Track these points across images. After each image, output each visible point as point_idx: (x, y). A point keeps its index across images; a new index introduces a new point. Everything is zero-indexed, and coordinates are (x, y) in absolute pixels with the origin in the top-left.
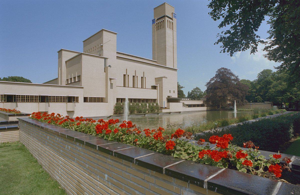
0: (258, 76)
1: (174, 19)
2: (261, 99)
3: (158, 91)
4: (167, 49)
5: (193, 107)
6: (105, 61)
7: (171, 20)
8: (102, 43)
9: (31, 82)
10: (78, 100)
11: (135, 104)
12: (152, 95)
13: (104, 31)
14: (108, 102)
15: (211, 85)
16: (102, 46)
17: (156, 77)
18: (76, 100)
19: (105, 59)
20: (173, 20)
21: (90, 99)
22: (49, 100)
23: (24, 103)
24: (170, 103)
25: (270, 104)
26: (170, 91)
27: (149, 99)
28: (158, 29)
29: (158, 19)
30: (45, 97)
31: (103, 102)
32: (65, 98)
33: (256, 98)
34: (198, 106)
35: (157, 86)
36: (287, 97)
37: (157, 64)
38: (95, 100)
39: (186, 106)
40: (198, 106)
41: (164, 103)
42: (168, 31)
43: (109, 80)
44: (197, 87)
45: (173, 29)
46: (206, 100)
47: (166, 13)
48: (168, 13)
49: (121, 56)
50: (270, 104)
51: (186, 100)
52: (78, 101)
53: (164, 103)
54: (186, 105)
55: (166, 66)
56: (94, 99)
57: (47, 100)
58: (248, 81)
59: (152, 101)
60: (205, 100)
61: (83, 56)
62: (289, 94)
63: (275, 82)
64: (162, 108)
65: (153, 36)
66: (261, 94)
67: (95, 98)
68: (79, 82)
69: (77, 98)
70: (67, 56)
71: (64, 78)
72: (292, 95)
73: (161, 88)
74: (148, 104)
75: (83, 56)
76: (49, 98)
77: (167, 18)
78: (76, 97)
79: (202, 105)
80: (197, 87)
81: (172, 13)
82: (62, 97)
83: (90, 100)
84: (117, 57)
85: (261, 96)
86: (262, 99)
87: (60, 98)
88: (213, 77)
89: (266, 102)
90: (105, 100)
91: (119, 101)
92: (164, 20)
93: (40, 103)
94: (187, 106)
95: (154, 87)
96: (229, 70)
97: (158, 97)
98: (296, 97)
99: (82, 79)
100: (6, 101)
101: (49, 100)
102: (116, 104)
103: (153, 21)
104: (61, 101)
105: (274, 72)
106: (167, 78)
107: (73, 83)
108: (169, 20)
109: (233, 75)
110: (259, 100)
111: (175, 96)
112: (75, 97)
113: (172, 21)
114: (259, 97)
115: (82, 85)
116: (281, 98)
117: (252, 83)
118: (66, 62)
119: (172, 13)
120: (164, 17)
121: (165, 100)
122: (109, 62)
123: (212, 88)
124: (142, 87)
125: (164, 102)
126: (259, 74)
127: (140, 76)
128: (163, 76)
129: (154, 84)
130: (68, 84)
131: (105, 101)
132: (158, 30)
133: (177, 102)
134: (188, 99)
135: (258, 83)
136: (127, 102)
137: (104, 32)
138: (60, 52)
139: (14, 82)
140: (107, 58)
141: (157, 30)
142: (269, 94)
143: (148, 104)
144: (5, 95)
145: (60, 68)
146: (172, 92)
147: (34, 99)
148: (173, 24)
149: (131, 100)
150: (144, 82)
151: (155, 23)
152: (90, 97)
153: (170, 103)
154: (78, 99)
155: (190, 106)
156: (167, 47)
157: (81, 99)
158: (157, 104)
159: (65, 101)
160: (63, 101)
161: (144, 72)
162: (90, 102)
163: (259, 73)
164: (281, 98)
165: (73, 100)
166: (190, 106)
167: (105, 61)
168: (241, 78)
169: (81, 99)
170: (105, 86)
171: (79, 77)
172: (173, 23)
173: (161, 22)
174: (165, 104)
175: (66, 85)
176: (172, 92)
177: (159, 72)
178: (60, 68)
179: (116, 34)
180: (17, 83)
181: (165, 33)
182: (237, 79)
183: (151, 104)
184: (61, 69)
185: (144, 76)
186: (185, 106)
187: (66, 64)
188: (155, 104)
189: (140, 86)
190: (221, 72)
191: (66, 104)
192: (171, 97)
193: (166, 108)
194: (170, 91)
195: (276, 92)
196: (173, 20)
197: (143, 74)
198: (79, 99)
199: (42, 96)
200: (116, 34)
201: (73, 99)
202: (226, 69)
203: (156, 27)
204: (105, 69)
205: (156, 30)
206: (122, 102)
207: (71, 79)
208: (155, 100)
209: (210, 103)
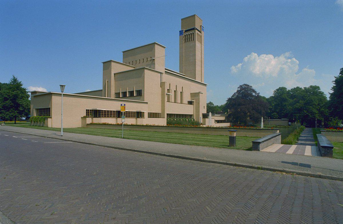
0: (274, 93)
1: (202, 32)
2: (277, 116)
4: (197, 63)
8: (154, 57)
10: (87, 112)
12: (189, 110)
16: (154, 60)
17: (192, 92)
18: (143, 116)
19: (161, 73)
23: (109, 118)
24: (206, 119)
25: (287, 120)
28: (186, 41)
29: (186, 31)
33: (273, 114)
35: (194, 101)
36: (304, 115)
42: (198, 44)
44: (210, 102)
47: (196, 25)
48: (197, 26)
50: (287, 120)
57: (99, 114)
62: (306, 112)
63: (291, 100)
65: (181, 48)
66: (278, 111)
71: (113, 92)
72: (309, 112)
78: (143, 112)
80: (210, 102)
81: (201, 26)
84: (165, 71)
85: (277, 113)
86: (278, 116)
88: (235, 93)
89: (283, 119)
91: (172, 117)
92: (193, 33)
94: (216, 122)
95: (190, 103)
96: (251, 86)
97: (194, 113)
98: (311, 115)
100: (93, 116)
103: (181, 33)
105: (289, 90)
106: (202, 93)
108: (199, 33)
109: (255, 92)
110: (275, 116)
112: (142, 112)
113: (200, 33)
114: (276, 113)
115: (145, 100)
116: (298, 115)
117: (267, 99)
118: (115, 74)
119: (201, 26)
120: (193, 29)
121: (201, 116)
123: (232, 103)
125: (201, 118)
126: (275, 91)
127: (179, 91)
129: (190, 100)
131: (161, 116)
135: (274, 100)
137: (156, 45)
141: (185, 42)
142: (287, 111)
148: (201, 38)
151: (183, 34)
157: (146, 115)
161: (176, 86)
163: (274, 90)
164: (298, 115)
168: (262, 95)
169: (146, 115)
170: (161, 102)
173: (190, 34)
177: (195, 88)
179: (165, 47)
182: (258, 97)
187: (115, 76)
190: (243, 89)
191: (135, 120)
195: (293, 109)
196: (201, 33)
197: (169, 87)
199: (137, 112)
200: (164, 47)
202: (248, 86)
203: (184, 39)
205: (184, 42)
208: (191, 116)
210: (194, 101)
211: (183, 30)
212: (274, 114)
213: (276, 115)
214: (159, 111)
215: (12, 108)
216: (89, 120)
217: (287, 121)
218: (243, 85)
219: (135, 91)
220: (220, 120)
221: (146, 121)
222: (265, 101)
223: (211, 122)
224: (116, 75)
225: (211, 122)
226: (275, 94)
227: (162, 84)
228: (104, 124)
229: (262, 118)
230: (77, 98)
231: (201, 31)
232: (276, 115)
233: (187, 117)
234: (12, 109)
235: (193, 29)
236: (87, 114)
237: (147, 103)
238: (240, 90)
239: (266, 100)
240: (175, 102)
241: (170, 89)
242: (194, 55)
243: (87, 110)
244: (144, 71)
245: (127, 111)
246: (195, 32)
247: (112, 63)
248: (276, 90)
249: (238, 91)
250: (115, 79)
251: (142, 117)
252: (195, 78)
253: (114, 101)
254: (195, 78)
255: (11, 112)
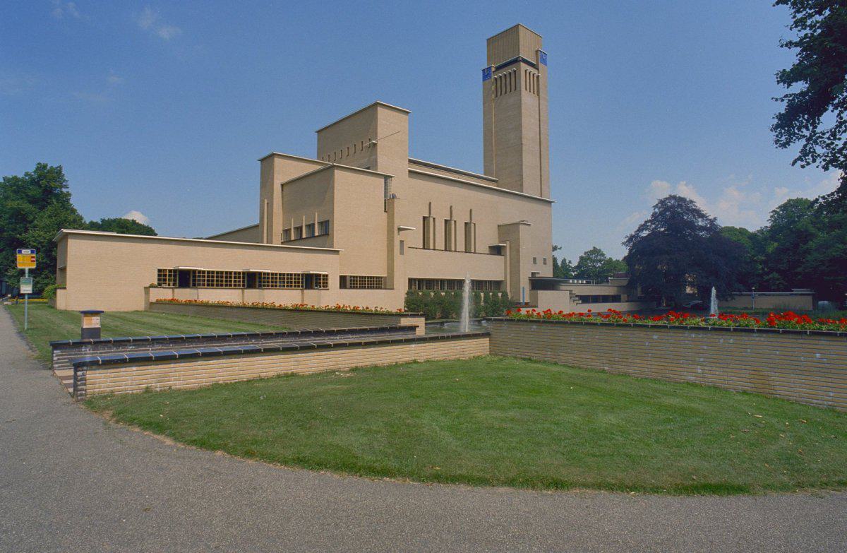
0: (771, 217)
1: (541, 66)
3: (505, 259)
4: (524, 148)
5: (603, 302)
6: (385, 183)
7: (533, 70)
8: (376, 138)
9: (156, 232)
11: (453, 293)
13: (379, 108)
14: (395, 287)
15: (639, 242)
18: (323, 283)
20: (538, 69)
21: (351, 281)
22: (264, 282)
26: (535, 259)
27: (486, 281)
28: (499, 94)
29: (498, 68)
30: (189, 275)
31: (381, 288)
32: (239, 278)
34: (605, 299)
35: (504, 246)
37: (497, 187)
38: (363, 284)
39: (577, 298)
40: (605, 299)
41: (523, 291)
42: (528, 99)
43: (396, 231)
45: (538, 95)
46: (628, 284)
49: (421, 171)
51: (578, 285)
52: (327, 286)
53: (523, 291)
54: (577, 296)
55: (522, 192)
56: (368, 281)
58: (742, 232)
59: (491, 287)
60: (625, 285)
61: (336, 171)
63: (822, 236)
64: (518, 306)
65: (486, 113)
67: (363, 277)
68: (323, 238)
69: (266, 276)
70: (285, 171)
71: (278, 228)
73: (517, 251)
74: (482, 294)
75: (336, 171)
76: (264, 278)
77: (523, 66)
78: (324, 275)
79: (615, 299)
80: (594, 248)
81: (537, 51)
82: (291, 275)
83: (351, 284)
84: (410, 171)
87: (288, 279)
88: (646, 222)
90: (385, 283)
92: (515, 71)
93: (176, 290)
95: (496, 250)
96: (691, 202)
99: (333, 230)
101: (264, 282)
102: (407, 294)
103: (486, 74)
104: (289, 286)
106: (530, 225)
107: (317, 236)
108: (529, 69)
109: (703, 216)
111: (547, 272)
112: (320, 275)
113: (536, 72)
114: (776, 275)
117: (752, 237)
118: (282, 185)
119: (537, 51)
120: (516, 61)
121: (525, 283)
122: (394, 187)
123: (641, 248)
124: (466, 250)
126: (774, 211)
127: (460, 219)
128: (517, 221)
129: (495, 242)
130: (288, 241)
132: (499, 96)
133: (553, 290)
134: (585, 282)
136: (467, 287)
138: (267, 161)
139: (122, 233)
140: (391, 177)
141: (496, 96)
143: (482, 294)
144: (175, 271)
145: (266, 201)
146: (540, 262)
147: (233, 279)
149: (477, 284)
150: (473, 234)
152: (351, 276)
153: (539, 292)
154: (327, 279)
155: (585, 299)
156: (524, 141)
157: (334, 282)
158: (505, 294)
159: (299, 286)
160: (226, 285)
162: (351, 288)
163: (774, 209)
165: (316, 283)
166: (585, 299)
167: (386, 184)
168: (723, 222)
169: (334, 282)
171: (326, 226)
172: (538, 77)
174: (525, 296)
175: (282, 243)
176: (540, 262)
177: (510, 210)
178: (266, 201)
179: (408, 113)
180: (142, 238)
181: (518, 106)
182: (712, 227)
183: (491, 294)
184: (270, 205)
185: (471, 219)
186: (574, 301)
187: (282, 190)
188: (500, 294)
189: (461, 247)
190: (667, 209)
191: (300, 294)
192: (537, 276)
193: (527, 305)
194: (535, 259)
196: (538, 69)
198: (330, 281)
201: (316, 279)
202: (683, 200)
203: (493, 87)
204: (385, 203)
206: (419, 289)
207: (299, 229)
208: (498, 284)
209: (639, 292)
210: (507, 245)
211: (490, 68)
212: (771, 276)
213: (778, 279)
214: (379, 271)
215: (46, 268)
216: (165, 294)
217: (810, 298)
218: (666, 199)
219: (318, 223)
220: (602, 296)
221: (332, 297)
222: (744, 241)
223: (557, 302)
224: (285, 188)
225: (557, 302)
226: (776, 220)
227: (389, 202)
228: (264, 308)
229: (714, 291)
230: (110, 243)
231: (538, 64)
232: (778, 279)
233: (484, 288)
234: (47, 272)
235: (516, 61)
236: (159, 280)
237: (338, 251)
238: (661, 214)
239: (748, 238)
240: (447, 249)
241: (451, 220)
242: (519, 128)
243: (160, 271)
244: (333, 174)
245: (269, 271)
246: (519, 69)
247: (277, 160)
248: (780, 207)
249: (654, 215)
250: (282, 197)
251: (320, 287)
252: (522, 185)
253: (166, 244)
254: (521, 187)
255: (46, 278)
